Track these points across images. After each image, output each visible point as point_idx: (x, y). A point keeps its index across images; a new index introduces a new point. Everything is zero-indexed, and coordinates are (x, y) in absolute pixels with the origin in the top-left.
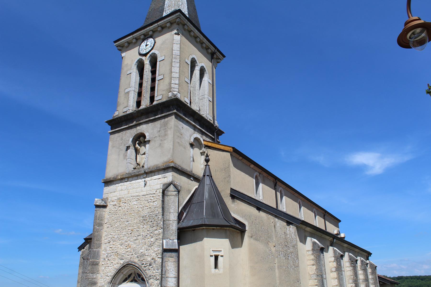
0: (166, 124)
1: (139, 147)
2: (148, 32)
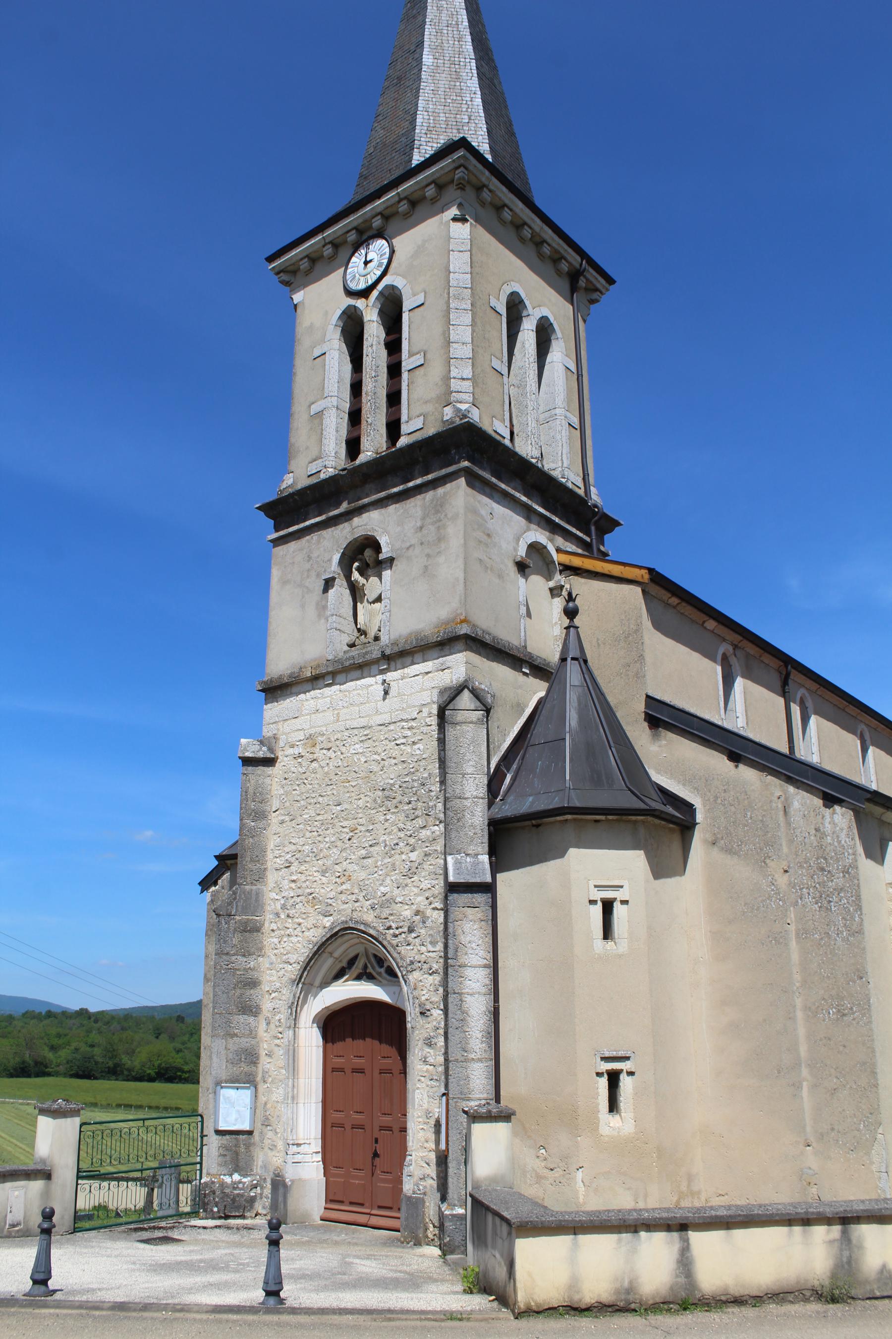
0: (439, 506)
1: (362, 580)
2: (368, 221)
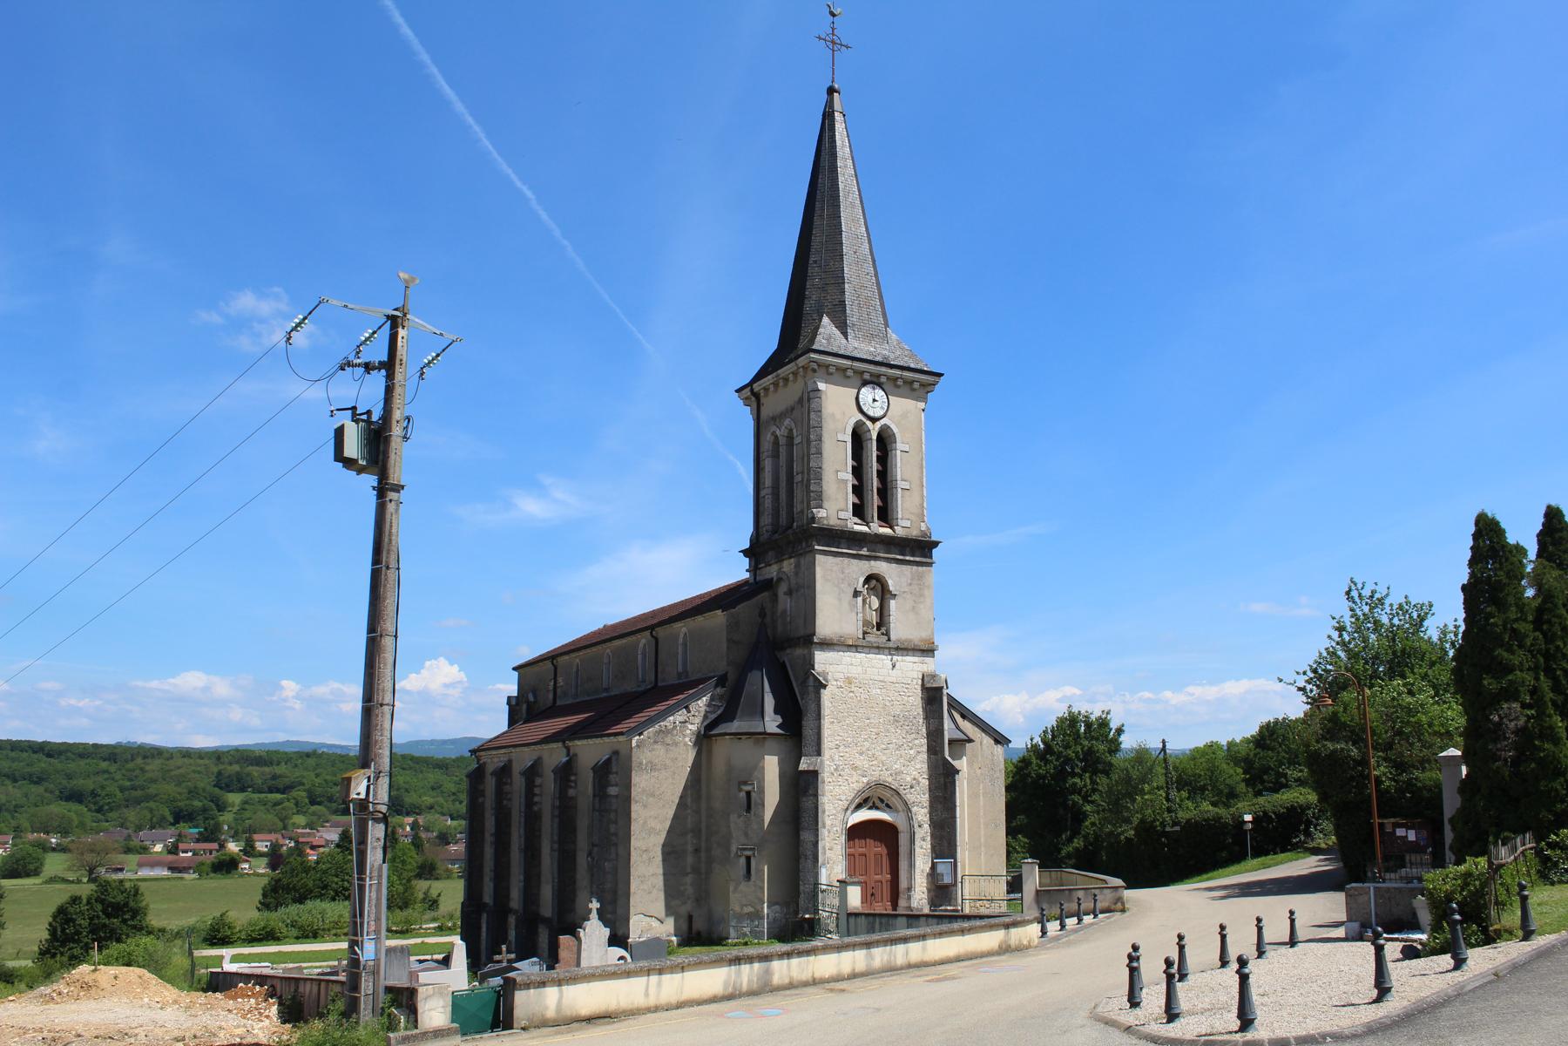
0: (920, 577)
2: (879, 376)
